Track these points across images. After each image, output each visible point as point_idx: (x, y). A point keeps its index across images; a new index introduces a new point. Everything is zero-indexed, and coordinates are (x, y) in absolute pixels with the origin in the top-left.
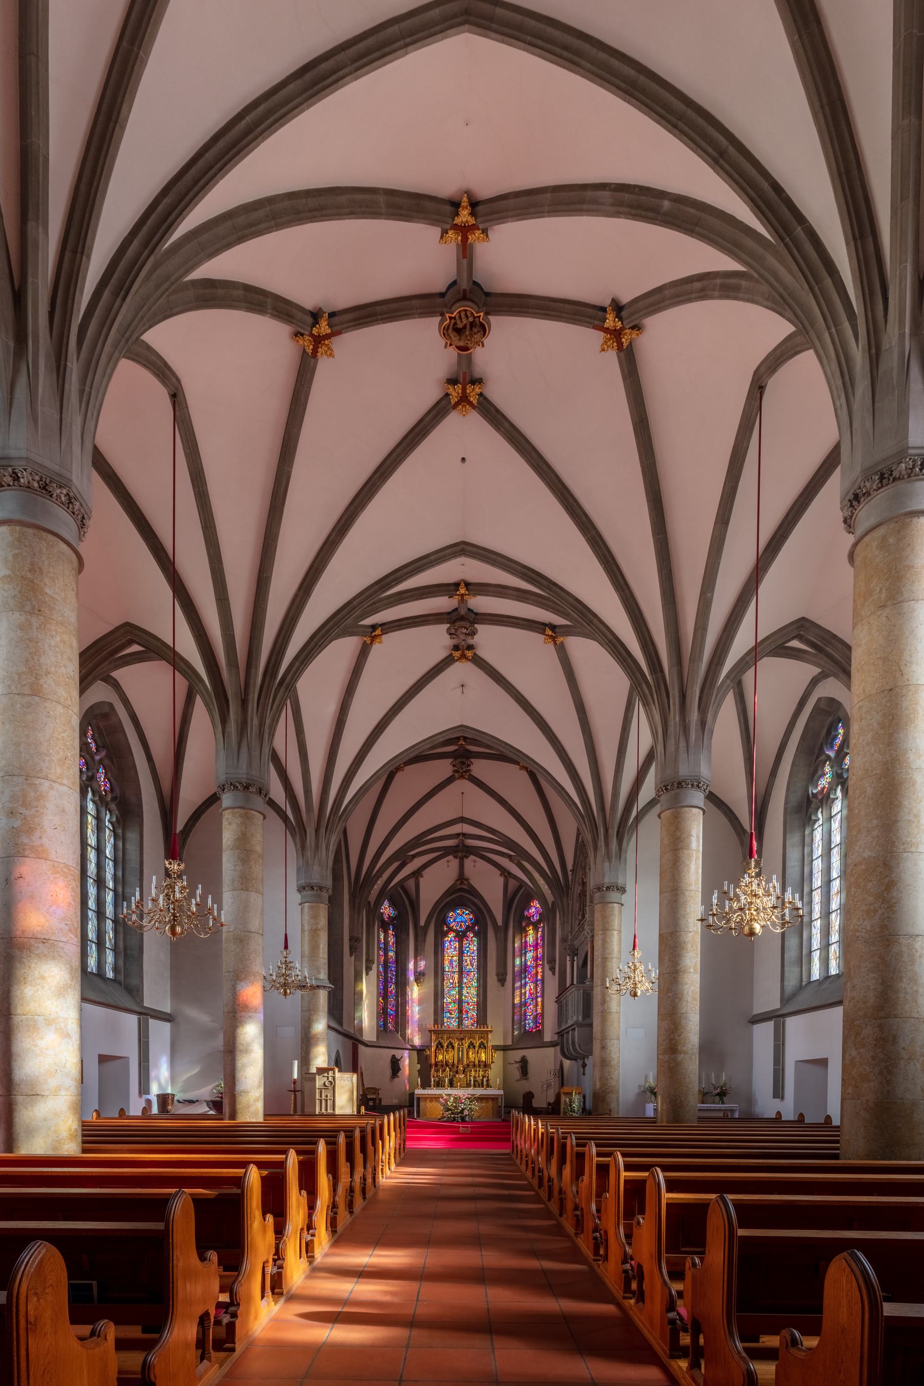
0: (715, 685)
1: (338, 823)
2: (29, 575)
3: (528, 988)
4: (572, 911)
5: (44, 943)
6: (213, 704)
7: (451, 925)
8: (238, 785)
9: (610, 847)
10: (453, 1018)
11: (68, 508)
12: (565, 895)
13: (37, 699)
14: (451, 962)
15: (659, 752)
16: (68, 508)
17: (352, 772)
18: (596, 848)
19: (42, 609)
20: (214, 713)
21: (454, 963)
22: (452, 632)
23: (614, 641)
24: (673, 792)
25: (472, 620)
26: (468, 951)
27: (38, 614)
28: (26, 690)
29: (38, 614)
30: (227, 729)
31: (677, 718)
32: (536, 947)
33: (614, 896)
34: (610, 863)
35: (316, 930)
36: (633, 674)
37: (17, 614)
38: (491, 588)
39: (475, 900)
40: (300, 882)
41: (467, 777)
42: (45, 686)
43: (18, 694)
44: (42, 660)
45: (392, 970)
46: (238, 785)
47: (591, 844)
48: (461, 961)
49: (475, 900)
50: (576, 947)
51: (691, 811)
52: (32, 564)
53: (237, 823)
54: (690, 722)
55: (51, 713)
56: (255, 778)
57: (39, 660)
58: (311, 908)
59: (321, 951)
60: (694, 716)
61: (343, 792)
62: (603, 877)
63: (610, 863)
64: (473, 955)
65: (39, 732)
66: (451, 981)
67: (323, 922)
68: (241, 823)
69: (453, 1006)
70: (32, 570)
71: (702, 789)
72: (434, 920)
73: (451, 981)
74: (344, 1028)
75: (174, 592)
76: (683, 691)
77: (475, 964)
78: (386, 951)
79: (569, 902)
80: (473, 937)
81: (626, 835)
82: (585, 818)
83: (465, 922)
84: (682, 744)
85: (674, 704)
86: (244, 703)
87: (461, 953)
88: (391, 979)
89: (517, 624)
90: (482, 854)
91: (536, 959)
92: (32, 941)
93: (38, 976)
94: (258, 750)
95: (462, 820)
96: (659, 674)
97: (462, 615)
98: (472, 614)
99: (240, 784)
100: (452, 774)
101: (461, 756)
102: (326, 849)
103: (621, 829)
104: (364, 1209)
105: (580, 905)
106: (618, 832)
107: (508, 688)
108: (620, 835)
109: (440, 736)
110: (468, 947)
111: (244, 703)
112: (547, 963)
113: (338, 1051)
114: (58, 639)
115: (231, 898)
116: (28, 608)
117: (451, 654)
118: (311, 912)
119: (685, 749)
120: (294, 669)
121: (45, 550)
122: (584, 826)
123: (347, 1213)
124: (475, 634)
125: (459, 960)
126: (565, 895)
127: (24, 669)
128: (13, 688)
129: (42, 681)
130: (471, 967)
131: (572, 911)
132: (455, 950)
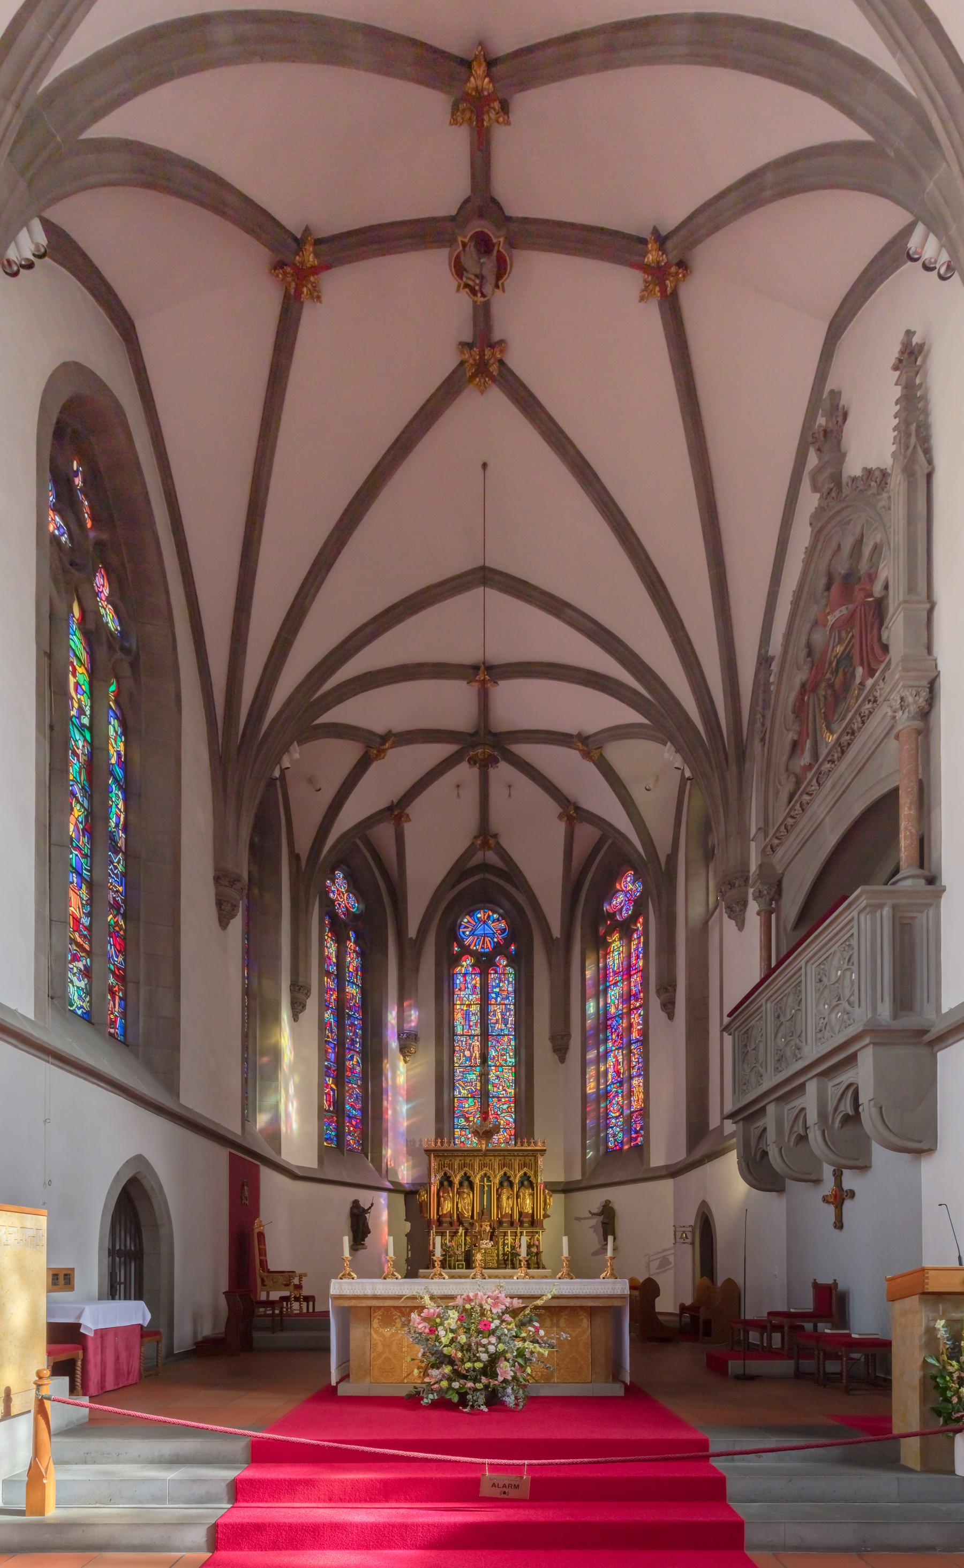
3: (611, 1060)
14: (467, 1016)
21: (473, 1018)
64: (507, 1002)
66: (467, 1053)
69: (470, 1105)
73: (467, 1053)
77: (511, 1020)
80: (506, 966)
110: (498, 986)
132: (474, 993)
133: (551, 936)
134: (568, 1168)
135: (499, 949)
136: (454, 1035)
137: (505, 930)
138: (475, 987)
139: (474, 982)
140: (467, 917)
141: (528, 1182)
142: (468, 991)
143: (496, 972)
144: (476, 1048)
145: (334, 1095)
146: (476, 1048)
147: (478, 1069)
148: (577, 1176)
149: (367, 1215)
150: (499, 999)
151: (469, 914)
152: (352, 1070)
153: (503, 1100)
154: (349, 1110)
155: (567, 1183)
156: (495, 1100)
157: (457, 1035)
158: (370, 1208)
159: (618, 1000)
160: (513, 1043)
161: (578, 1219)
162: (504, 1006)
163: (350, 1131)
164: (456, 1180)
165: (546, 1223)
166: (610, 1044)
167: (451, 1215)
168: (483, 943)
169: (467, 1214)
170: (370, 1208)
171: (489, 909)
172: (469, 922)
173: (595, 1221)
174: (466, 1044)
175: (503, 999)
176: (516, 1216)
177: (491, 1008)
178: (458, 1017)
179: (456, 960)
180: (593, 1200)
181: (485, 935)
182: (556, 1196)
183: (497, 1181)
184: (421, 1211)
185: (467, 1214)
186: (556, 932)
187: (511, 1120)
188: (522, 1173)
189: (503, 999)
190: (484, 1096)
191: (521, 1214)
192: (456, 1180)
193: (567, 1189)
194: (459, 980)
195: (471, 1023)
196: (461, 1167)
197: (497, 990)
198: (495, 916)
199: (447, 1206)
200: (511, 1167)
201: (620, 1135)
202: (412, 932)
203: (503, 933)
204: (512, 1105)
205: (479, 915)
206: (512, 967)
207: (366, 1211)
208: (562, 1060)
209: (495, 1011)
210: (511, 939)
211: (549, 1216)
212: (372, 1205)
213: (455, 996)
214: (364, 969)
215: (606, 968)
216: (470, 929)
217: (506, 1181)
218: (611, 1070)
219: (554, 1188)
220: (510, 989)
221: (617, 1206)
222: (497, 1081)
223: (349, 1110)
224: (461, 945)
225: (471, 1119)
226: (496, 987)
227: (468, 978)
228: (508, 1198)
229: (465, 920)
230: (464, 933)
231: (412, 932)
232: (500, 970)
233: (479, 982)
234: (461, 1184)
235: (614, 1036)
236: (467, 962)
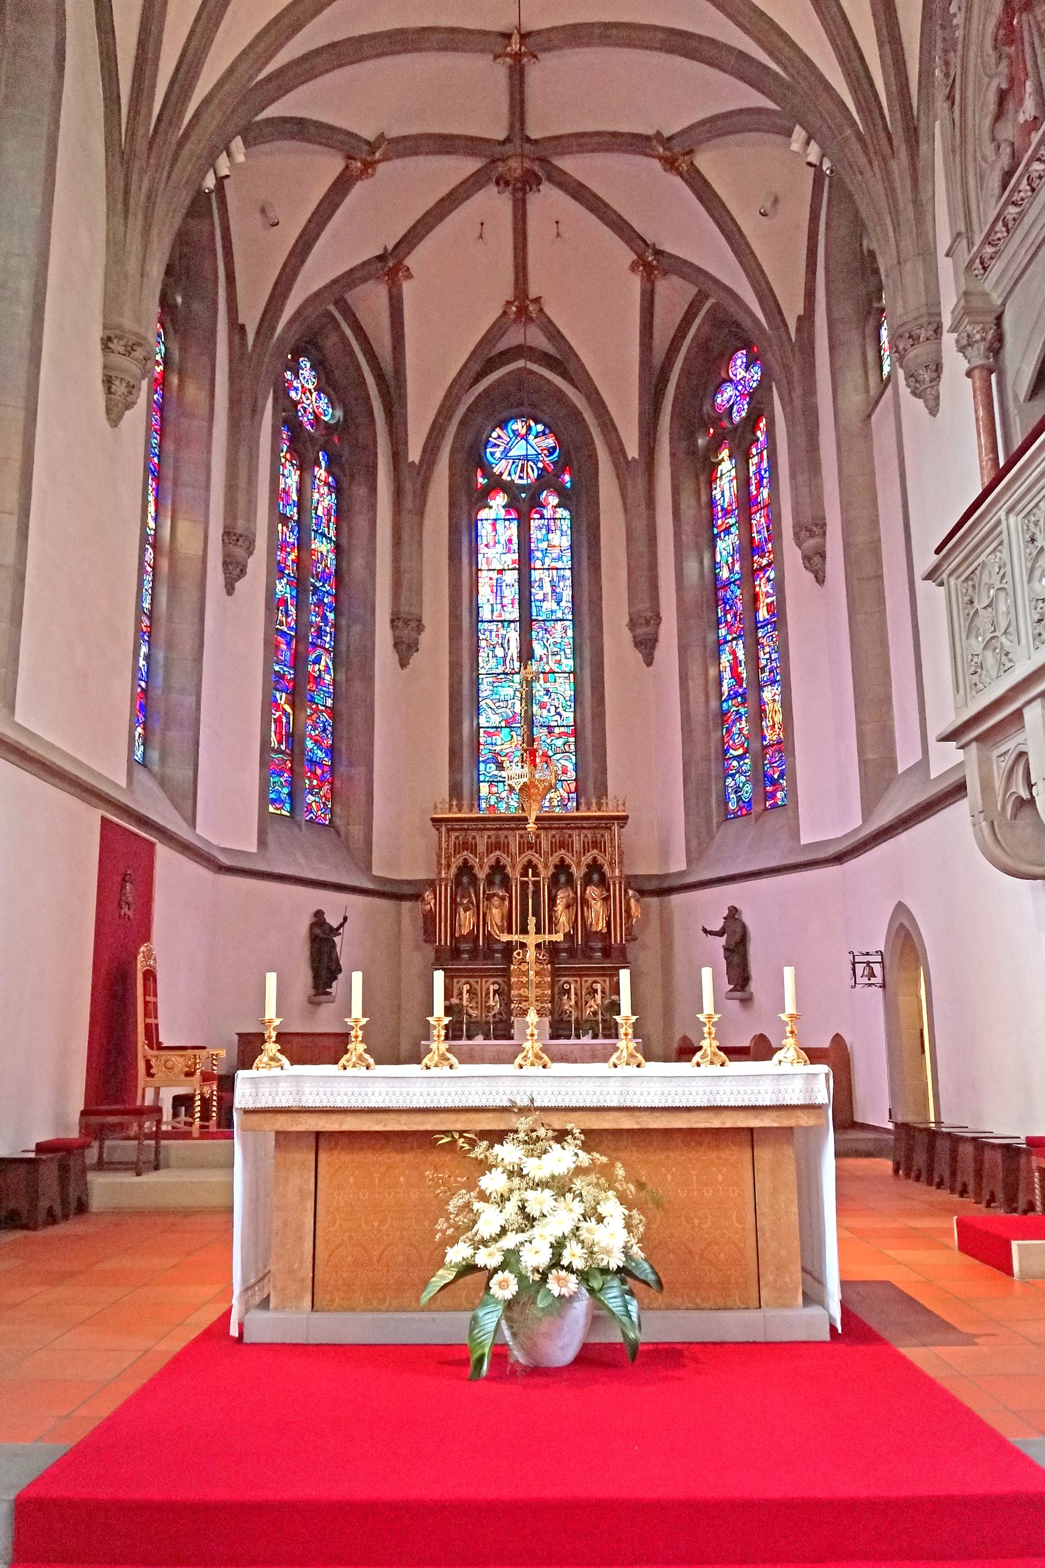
3: (726, 658)
14: (497, 589)
48: (525, 584)
64: (559, 565)
77: (567, 595)
80: (558, 506)
130: (555, 606)
133: (625, 457)
135: (546, 480)
136: (478, 621)
137: (554, 448)
138: (510, 541)
139: (508, 533)
140: (498, 430)
142: (500, 548)
143: (542, 517)
145: (288, 723)
150: (547, 561)
152: (318, 680)
154: (311, 750)
157: (482, 621)
158: (342, 925)
159: (733, 556)
160: (570, 633)
162: (555, 572)
163: (312, 787)
166: (723, 632)
168: (522, 471)
170: (342, 925)
172: (499, 437)
174: (497, 636)
177: (535, 575)
178: (485, 592)
181: (526, 458)
186: (633, 451)
194: (485, 530)
195: (505, 601)
197: (544, 545)
198: (540, 428)
201: (748, 788)
202: (414, 455)
203: (551, 454)
205: (515, 427)
206: (566, 508)
209: (541, 579)
210: (564, 464)
212: (345, 919)
213: (480, 556)
214: (341, 513)
215: (712, 503)
216: (501, 449)
218: (727, 675)
220: (566, 542)
221: (747, 918)
223: (311, 750)
224: (487, 470)
230: (492, 454)
231: (414, 455)
232: (548, 513)
235: (729, 617)
236: (499, 500)
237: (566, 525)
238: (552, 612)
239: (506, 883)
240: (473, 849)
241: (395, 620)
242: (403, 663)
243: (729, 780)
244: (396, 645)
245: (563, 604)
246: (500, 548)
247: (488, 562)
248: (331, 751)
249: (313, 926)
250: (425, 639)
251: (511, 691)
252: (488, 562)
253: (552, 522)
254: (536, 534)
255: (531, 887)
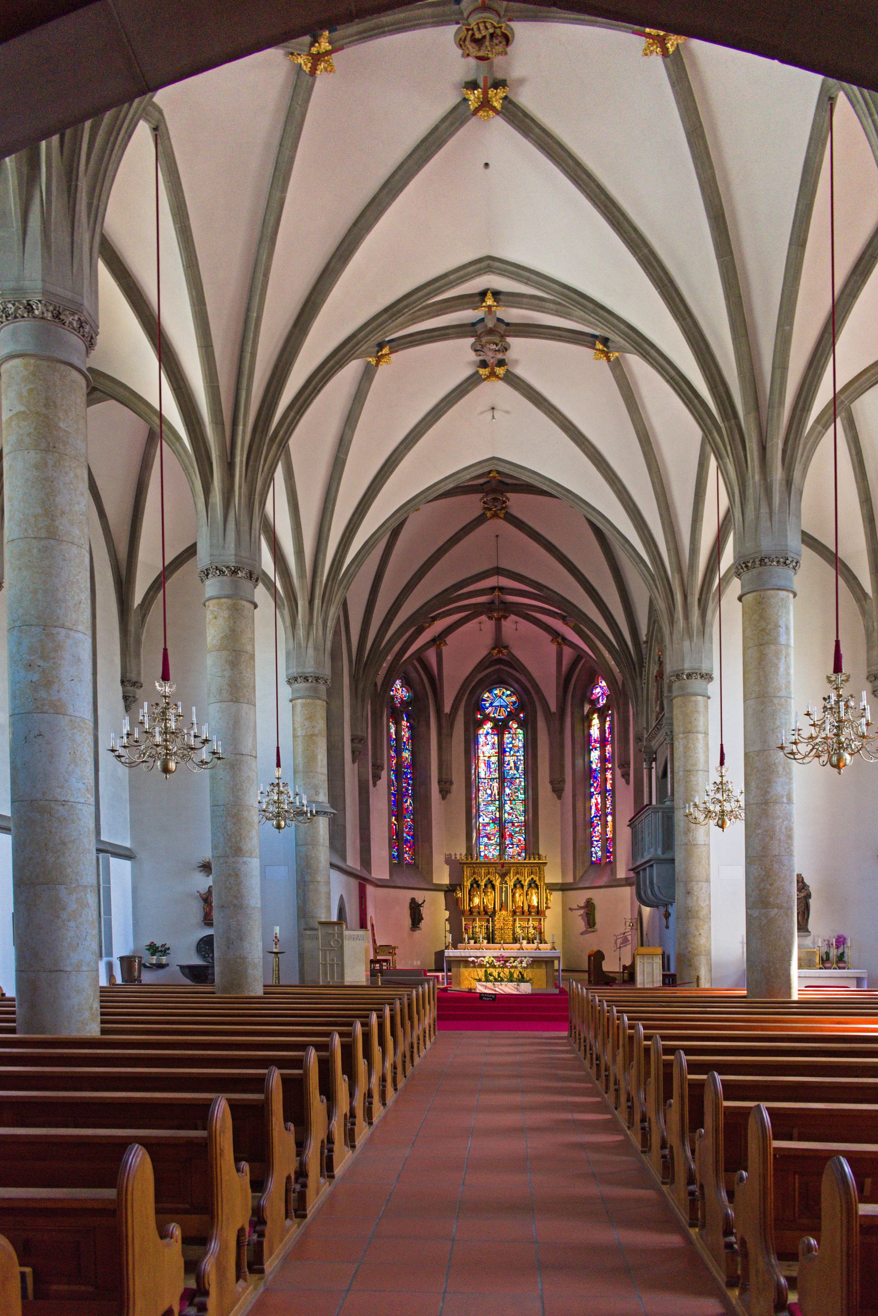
0: (801, 435)
1: (338, 590)
2: (44, 411)
4: (648, 699)
5: (64, 805)
6: (195, 474)
7: (487, 711)
8: (224, 569)
9: (690, 620)
10: (492, 845)
11: (79, 332)
12: (638, 674)
13: (52, 542)
14: (488, 765)
15: (736, 520)
16: (79, 332)
17: (355, 525)
18: (672, 621)
19: (57, 445)
20: (194, 477)
21: (492, 766)
22: (478, 348)
23: (677, 378)
24: (755, 571)
25: (502, 332)
26: (511, 749)
27: (53, 451)
28: (43, 534)
29: (53, 451)
30: (211, 500)
31: (757, 477)
32: (603, 741)
33: (696, 684)
34: (691, 641)
35: (312, 735)
36: (702, 418)
37: (32, 453)
38: (525, 300)
39: (518, 675)
40: (290, 671)
41: (502, 516)
42: (61, 527)
43: (34, 538)
44: (58, 499)
45: (407, 778)
46: (224, 569)
47: (665, 616)
48: (501, 763)
49: (518, 675)
50: (654, 748)
51: (778, 594)
52: (47, 399)
53: (224, 618)
54: (771, 481)
55: (66, 555)
56: (246, 560)
57: (54, 500)
58: (304, 705)
59: (320, 764)
60: (778, 473)
61: (343, 550)
62: (683, 660)
63: (691, 641)
64: (518, 754)
65: (56, 577)
66: (489, 792)
67: (321, 725)
68: (229, 617)
69: (492, 829)
70: (47, 405)
71: (791, 566)
72: (463, 703)
73: (489, 792)
74: (348, 863)
75: (160, 362)
76: (762, 443)
77: (521, 767)
78: (399, 752)
79: (643, 685)
80: (517, 728)
81: (710, 601)
82: (657, 581)
83: (506, 707)
84: (764, 510)
85: (752, 460)
86: (229, 466)
87: (502, 751)
88: (407, 790)
89: (560, 336)
90: (527, 614)
91: (603, 759)
92: (53, 805)
93: (59, 842)
94: (247, 524)
95: (498, 571)
96: (733, 422)
97: (491, 328)
98: (502, 325)
99: (227, 567)
100: (482, 512)
101: (494, 491)
102: (323, 626)
103: (704, 596)
104: (396, 1102)
105: (657, 692)
106: (699, 600)
107: (552, 413)
108: (702, 605)
109: (466, 472)
110: (511, 743)
111: (229, 466)
112: (619, 766)
113: (341, 896)
114: (72, 475)
115: (219, 711)
116: (43, 446)
117: (477, 372)
118: (306, 712)
119: (768, 515)
120: (288, 420)
121: (58, 382)
122: (656, 591)
123: (381, 1105)
124: (506, 349)
125: (498, 761)
126: (638, 674)
127: (40, 511)
128: (30, 532)
129: (57, 523)
130: (516, 772)
131: (648, 699)
132: (493, 748)
134: (564, 873)
135: (511, 716)
137: (515, 702)
139: (493, 740)
141: (533, 884)
142: (489, 747)
143: (510, 733)
144: (495, 788)
146: (495, 788)
147: (497, 803)
148: (570, 879)
149: (421, 908)
150: (512, 753)
151: (488, 691)
153: (516, 824)
155: (562, 884)
156: (511, 824)
160: (523, 784)
161: (571, 909)
164: (483, 884)
165: (547, 912)
167: (479, 907)
169: (491, 907)
171: (503, 688)
172: (488, 697)
173: (581, 912)
175: (515, 752)
176: (526, 908)
177: (507, 759)
179: (480, 724)
180: (580, 898)
181: (501, 706)
182: (554, 893)
183: (512, 884)
184: (457, 904)
185: (491, 907)
187: (522, 839)
188: (530, 878)
189: (515, 752)
190: (500, 822)
191: (529, 906)
192: (483, 884)
193: (563, 888)
194: (482, 740)
195: (492, 770)
196: (486, 875)
197: (511, 746)
198: (509, 692)
199: (476, 901)
200: (522, 874)
204: (523, 828)
205: (496, 692)
206: (521, 729)
207: (420, 906)
208: (559, 797)
211: (549, 908)
212: (424, 901)
217: (518, 884)
219: (552, 887)
220: (521, 745)
221: (595, 902)
222: (511, 811)
225: (492, 838)
226: (509, 744)
227: (489, 737)
228: (520, 895)
229: (486, 696)
233: (497, 740)
234: (486, 885)
236: (488, 726)
237: (521, 737)
238: (515, 774)
239: (493, 887)
240: (480, 874)
241: (439, 782)
242: (444, 798)
243: (593, 849)
244: (440, 791)
245: (520, 771)
246: (489, 747)
247: (483, 753)
248: (413, 837)
249: (411, 903)
250: (454, 788)
251: (494, 808)
252: (483, 753)
253: (514, 736)
254: (506, 741)
255: (504, 889)
